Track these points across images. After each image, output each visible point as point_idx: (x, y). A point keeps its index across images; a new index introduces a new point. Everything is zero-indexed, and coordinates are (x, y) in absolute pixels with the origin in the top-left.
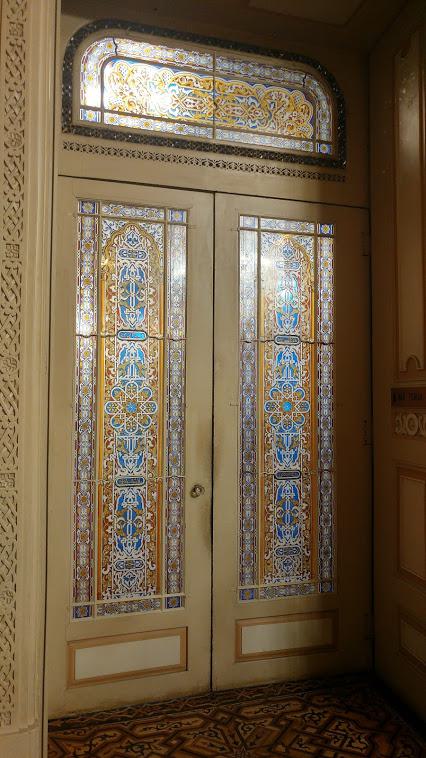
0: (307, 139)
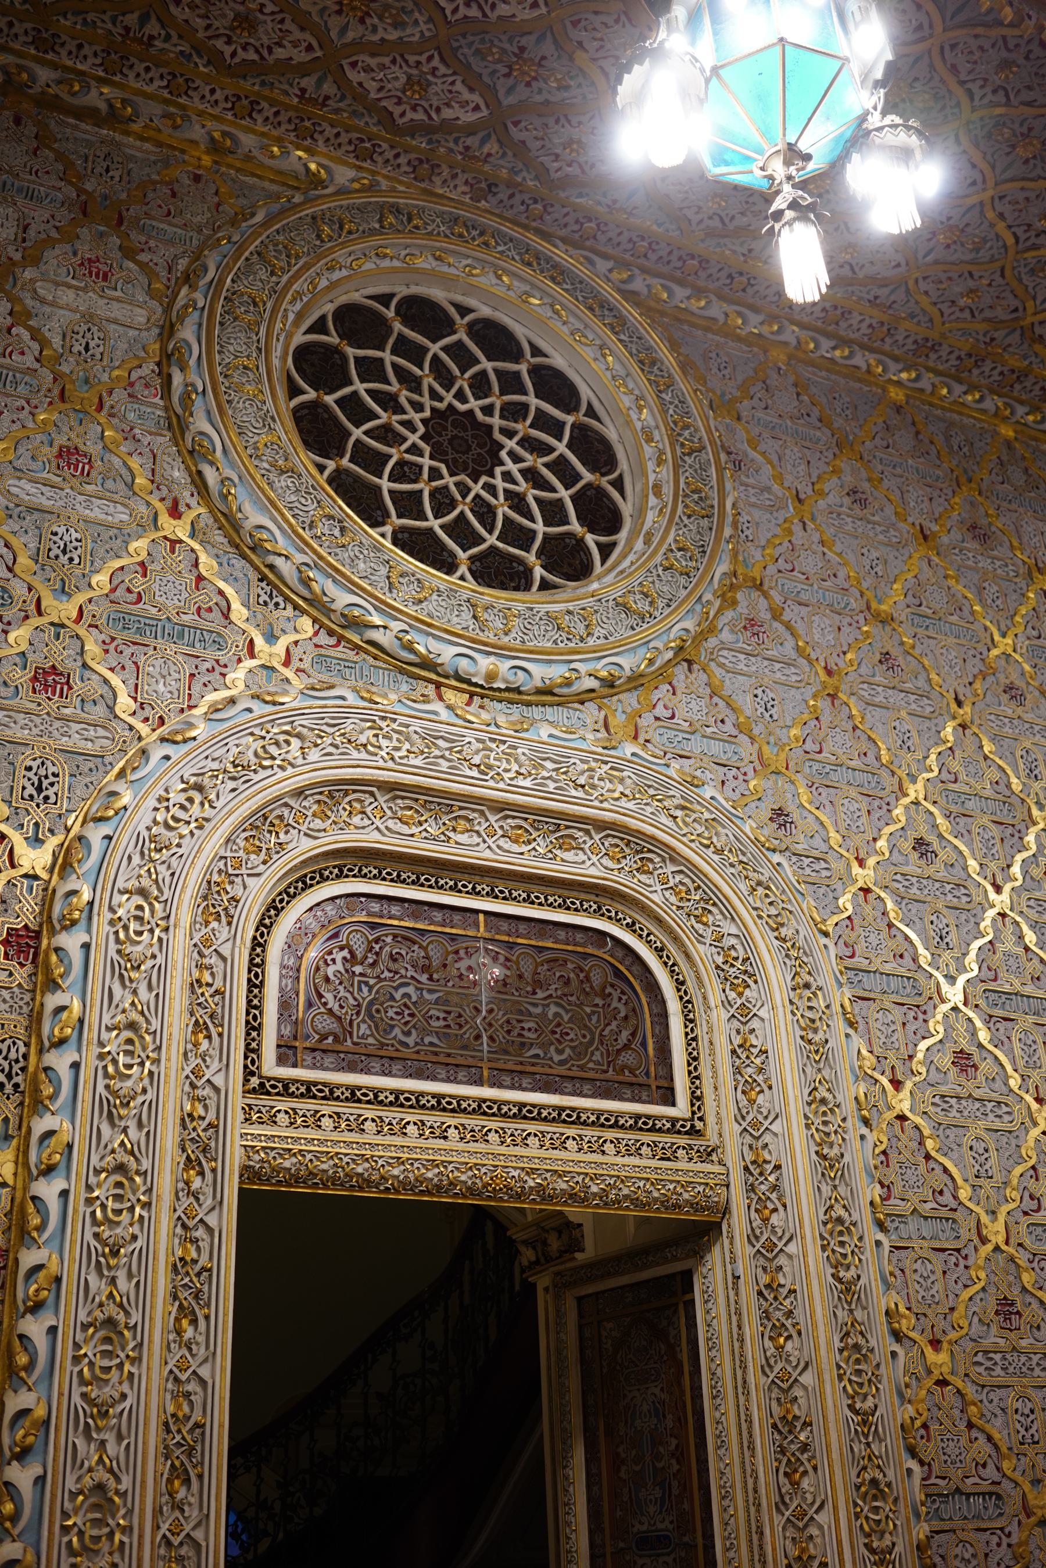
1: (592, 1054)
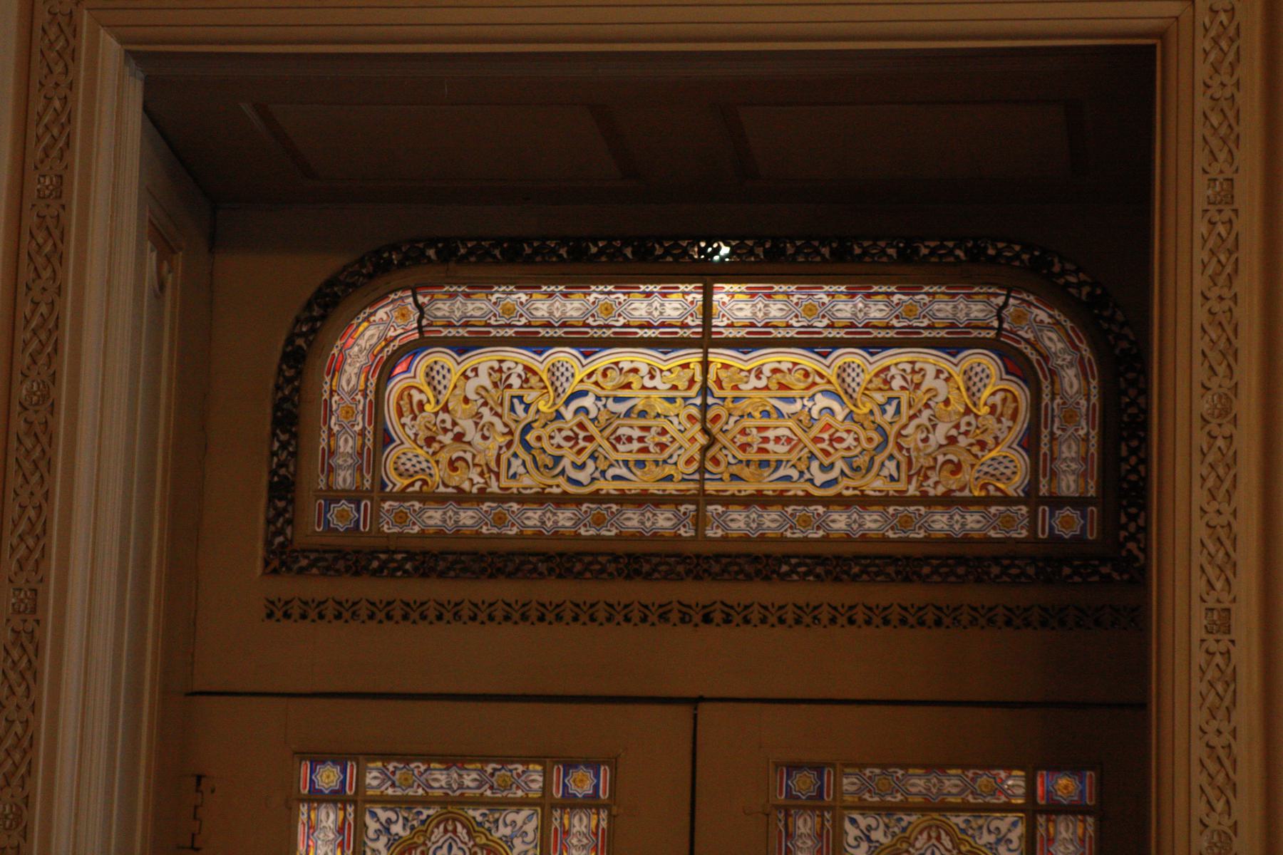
0: (1006, 500)
1: (883, 465)
